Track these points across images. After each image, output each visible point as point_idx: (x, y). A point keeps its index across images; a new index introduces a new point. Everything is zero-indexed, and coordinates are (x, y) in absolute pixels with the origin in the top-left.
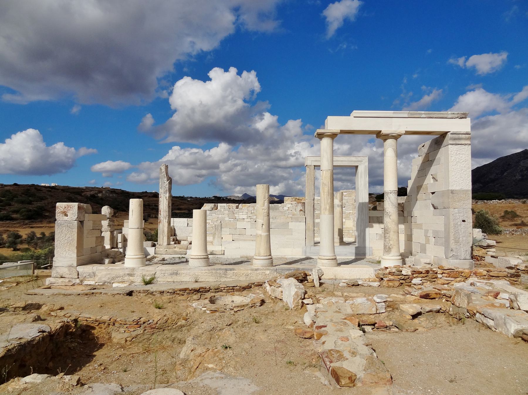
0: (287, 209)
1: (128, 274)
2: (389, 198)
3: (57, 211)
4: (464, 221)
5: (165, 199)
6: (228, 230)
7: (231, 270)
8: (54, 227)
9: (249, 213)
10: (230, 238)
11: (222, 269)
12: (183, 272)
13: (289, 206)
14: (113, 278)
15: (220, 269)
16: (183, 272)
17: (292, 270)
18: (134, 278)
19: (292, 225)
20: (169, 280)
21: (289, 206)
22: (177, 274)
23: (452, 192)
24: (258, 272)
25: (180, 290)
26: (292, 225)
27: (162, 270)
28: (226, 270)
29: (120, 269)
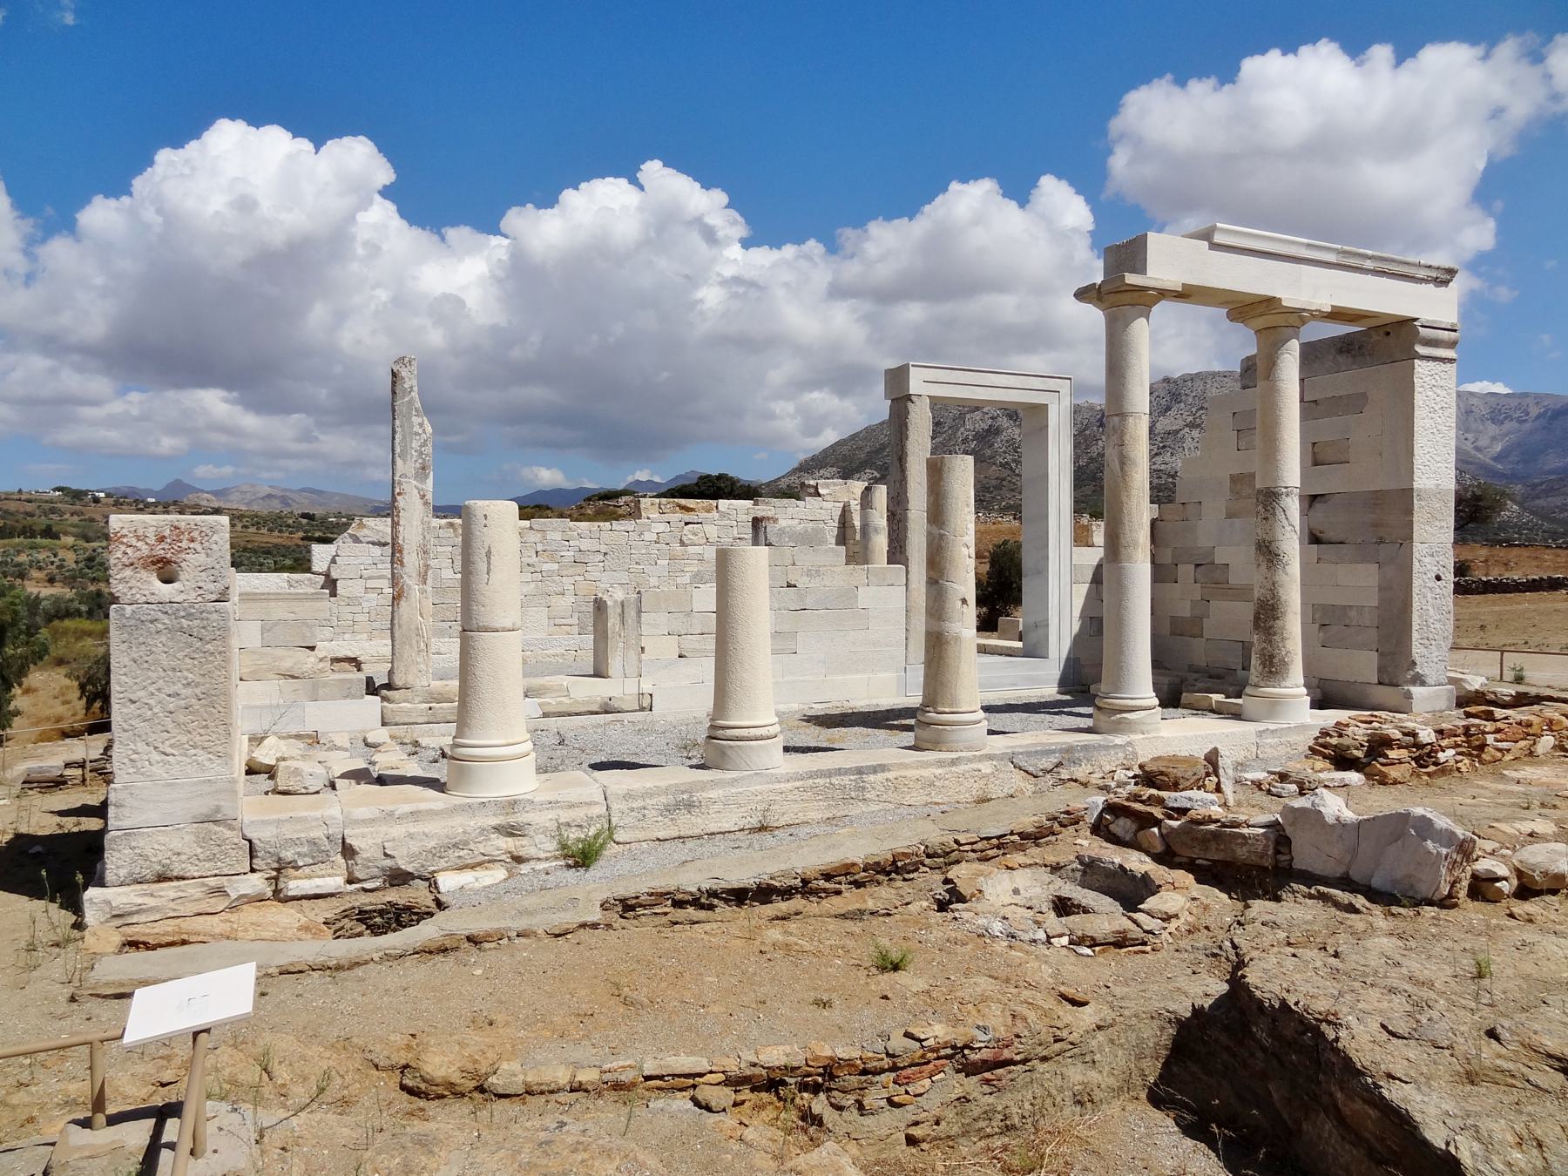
0: (655, 537)
1: (497, 829)
3: (116, 556)
4: (1438, 578)
5: (418, 502)
6: (662, 618)
7: (875, 770)
8: (105, 633)
9: (526, 553)
10: (670, 647)
11: (847, 772)
12: (713, 794)
13: (662, 527)
14: (435, 854)
15: (839, 772)
16: (713, 794)
17: (1054, 752)
18: (524, 841)
19: (866, 596)
20: (661, 835)
21: (662, 527)
22: (690, 806)
24: (962, 768)
25: (828, 877)
26: (866, 596)
27: (628, 796)
28: (860, 771)
29: (454, 810)
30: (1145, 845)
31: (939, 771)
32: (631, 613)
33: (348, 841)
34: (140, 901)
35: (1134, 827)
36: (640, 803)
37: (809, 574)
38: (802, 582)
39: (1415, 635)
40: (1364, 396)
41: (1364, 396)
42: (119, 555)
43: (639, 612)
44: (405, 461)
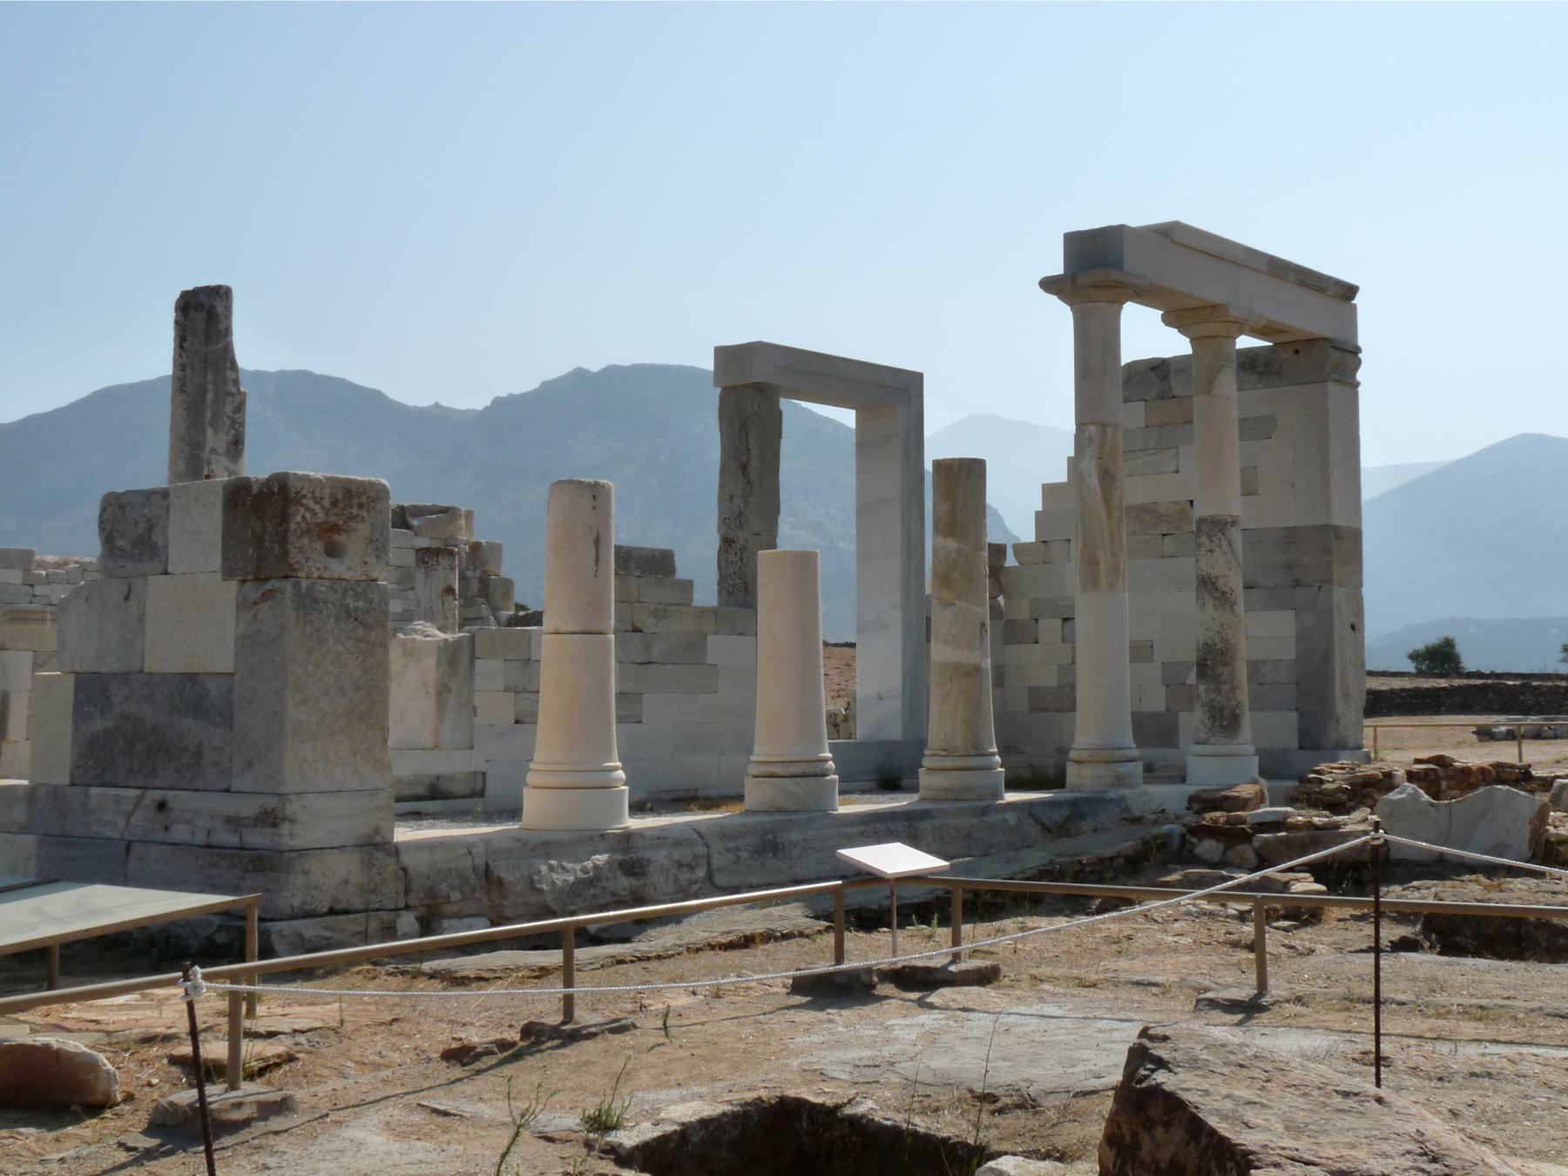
2: (1230, 544)
12: (794, 836)
23: (1336, 528)
30: (1237, 861)
31: (975, 821)
32: (465, 658)
33: (496, 873)
34: (327, 934)
35: (1221, 846)
36: (731, 844)
37: (655, 614)
38: (649, 625)
39: (1338, 693)
40: (1272, 420)
41: (1272, 420)
42: (299, 518)
43: (473, 658)
44: (215, 432)
